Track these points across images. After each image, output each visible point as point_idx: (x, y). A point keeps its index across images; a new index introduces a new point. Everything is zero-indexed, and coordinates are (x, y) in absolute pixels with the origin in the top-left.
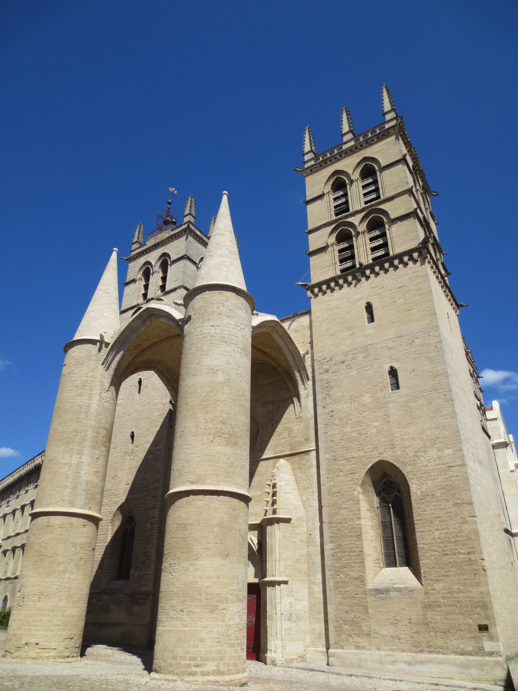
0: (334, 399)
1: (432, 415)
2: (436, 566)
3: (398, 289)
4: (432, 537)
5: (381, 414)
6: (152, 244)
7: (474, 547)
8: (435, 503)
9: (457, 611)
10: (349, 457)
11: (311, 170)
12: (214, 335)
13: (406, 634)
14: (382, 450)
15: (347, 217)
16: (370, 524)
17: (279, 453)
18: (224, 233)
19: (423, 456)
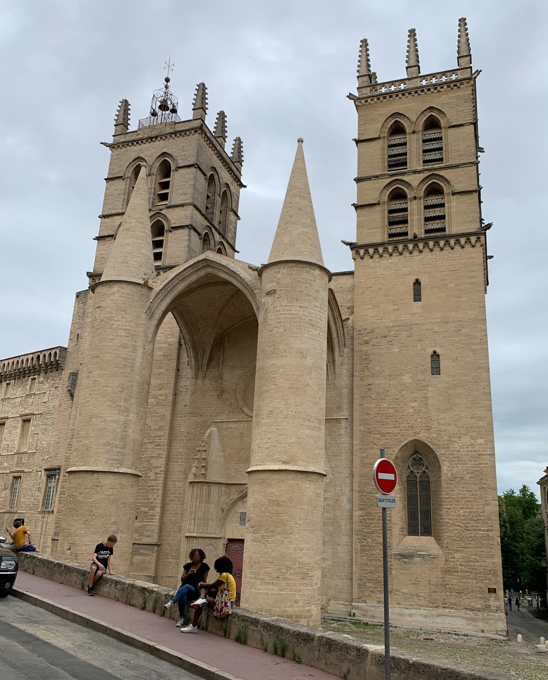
0: (373, 372)
1: (470, 405)
2: (458, 539)
3: (451, 272)
4: (457, 514)
5: (419, 396)
6: (146, 136)
7: (493, 526)
8: (463, 485)
9: (472, 576)
10: (384, 432)
11: (366, 101)
12: (303, 317)
13: (425, 593)
14: (417, 431)
15: (404, 174)
16: (399, 496)
18: (305, 195)
19: (457, 442)
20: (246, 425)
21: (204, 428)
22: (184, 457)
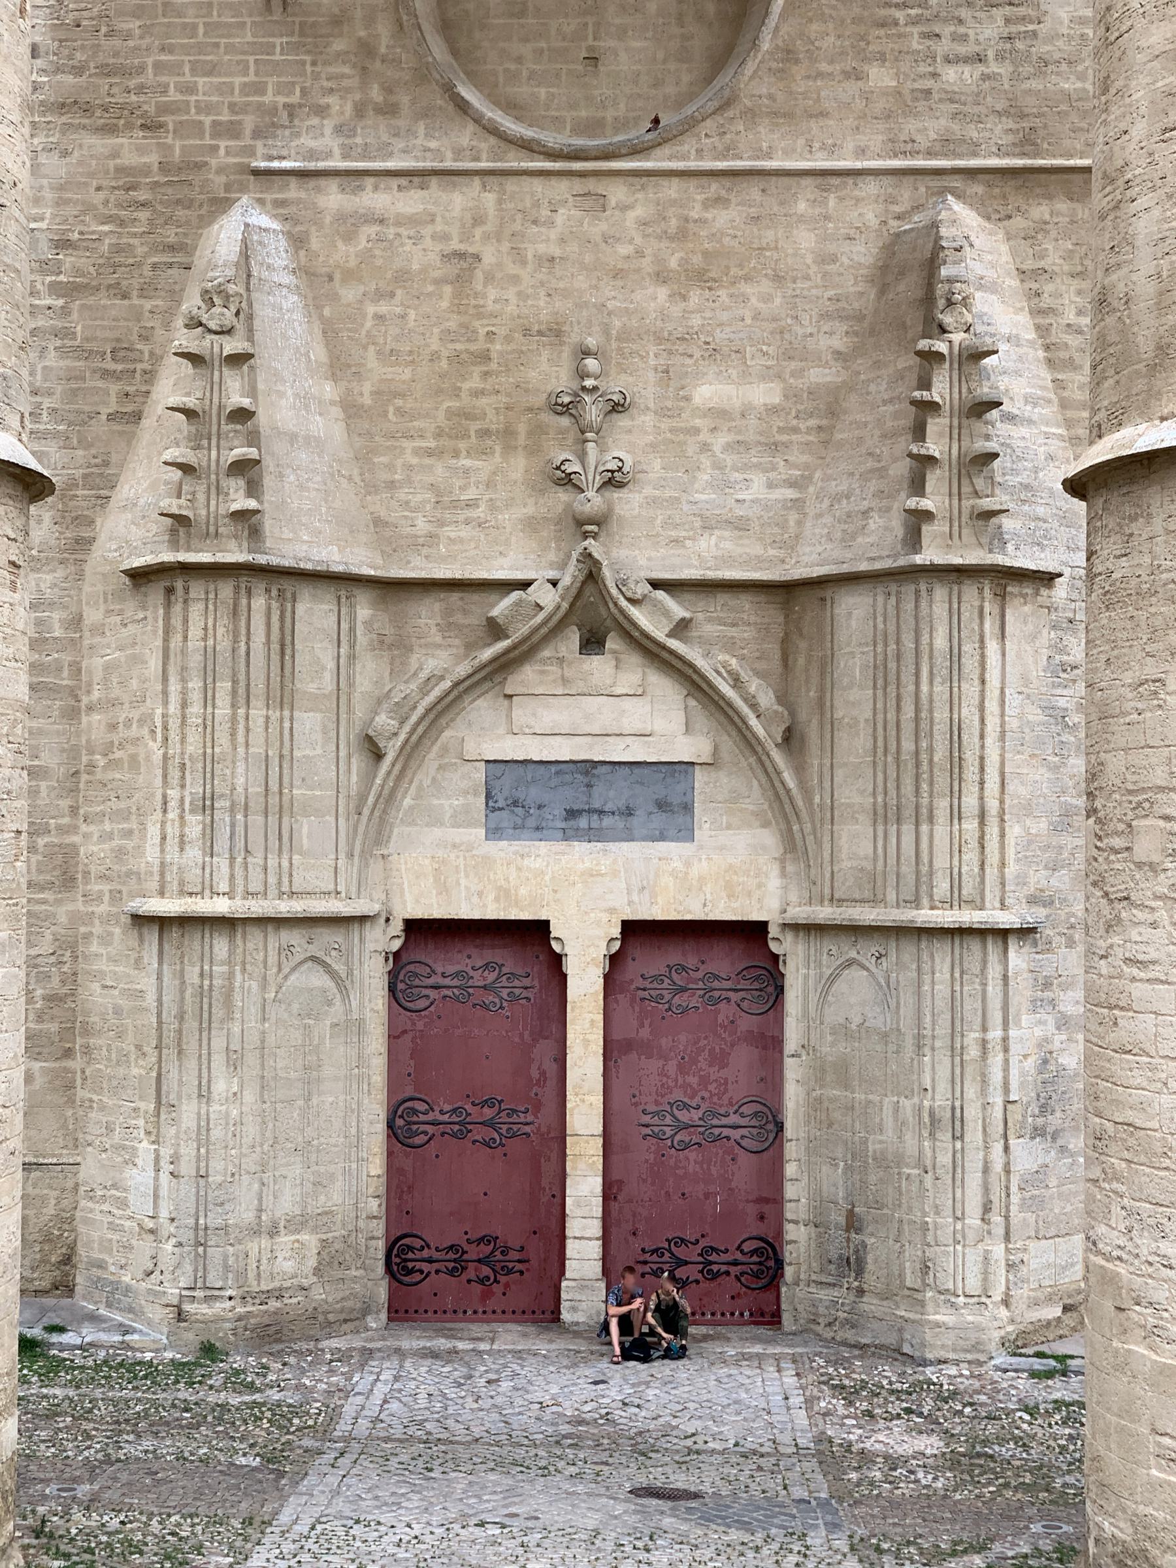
17: (930, 154)
20: (489, 199)
21: (181, 213)
22: (47, 403)
